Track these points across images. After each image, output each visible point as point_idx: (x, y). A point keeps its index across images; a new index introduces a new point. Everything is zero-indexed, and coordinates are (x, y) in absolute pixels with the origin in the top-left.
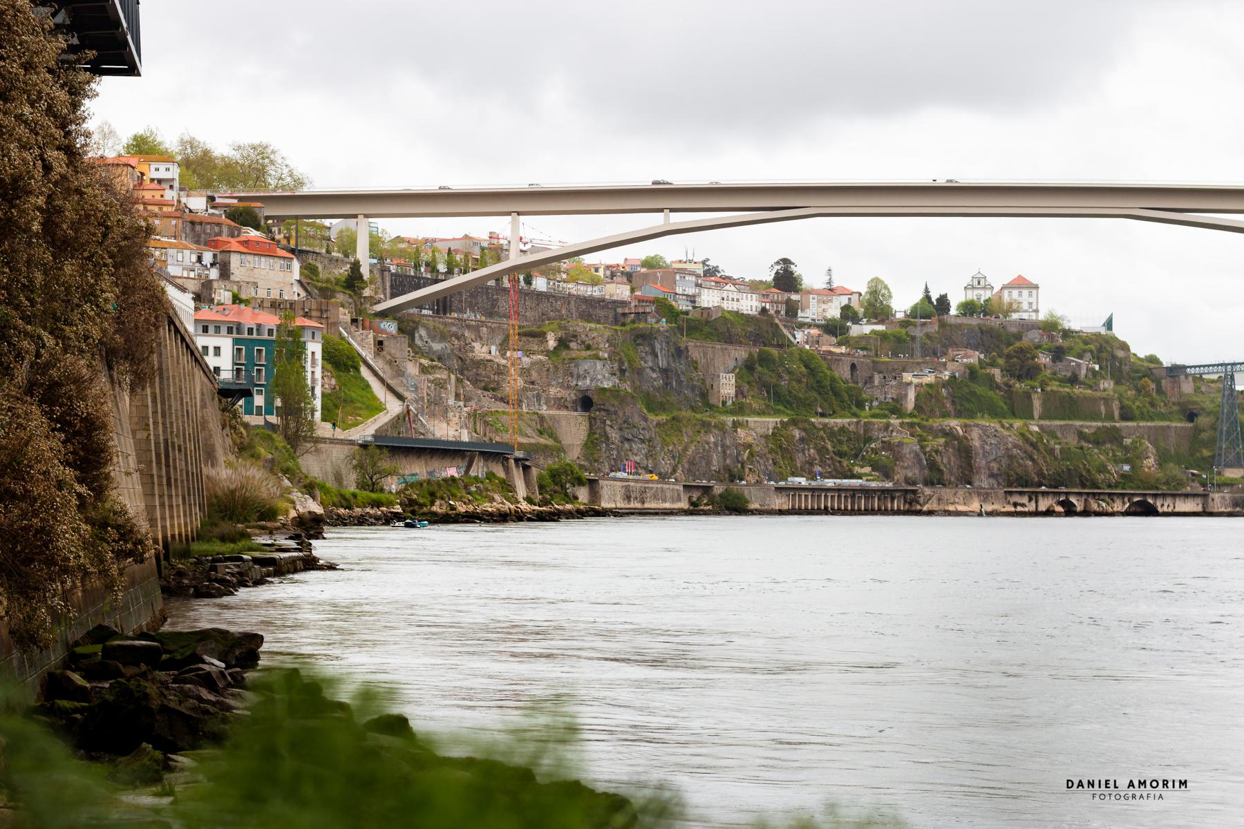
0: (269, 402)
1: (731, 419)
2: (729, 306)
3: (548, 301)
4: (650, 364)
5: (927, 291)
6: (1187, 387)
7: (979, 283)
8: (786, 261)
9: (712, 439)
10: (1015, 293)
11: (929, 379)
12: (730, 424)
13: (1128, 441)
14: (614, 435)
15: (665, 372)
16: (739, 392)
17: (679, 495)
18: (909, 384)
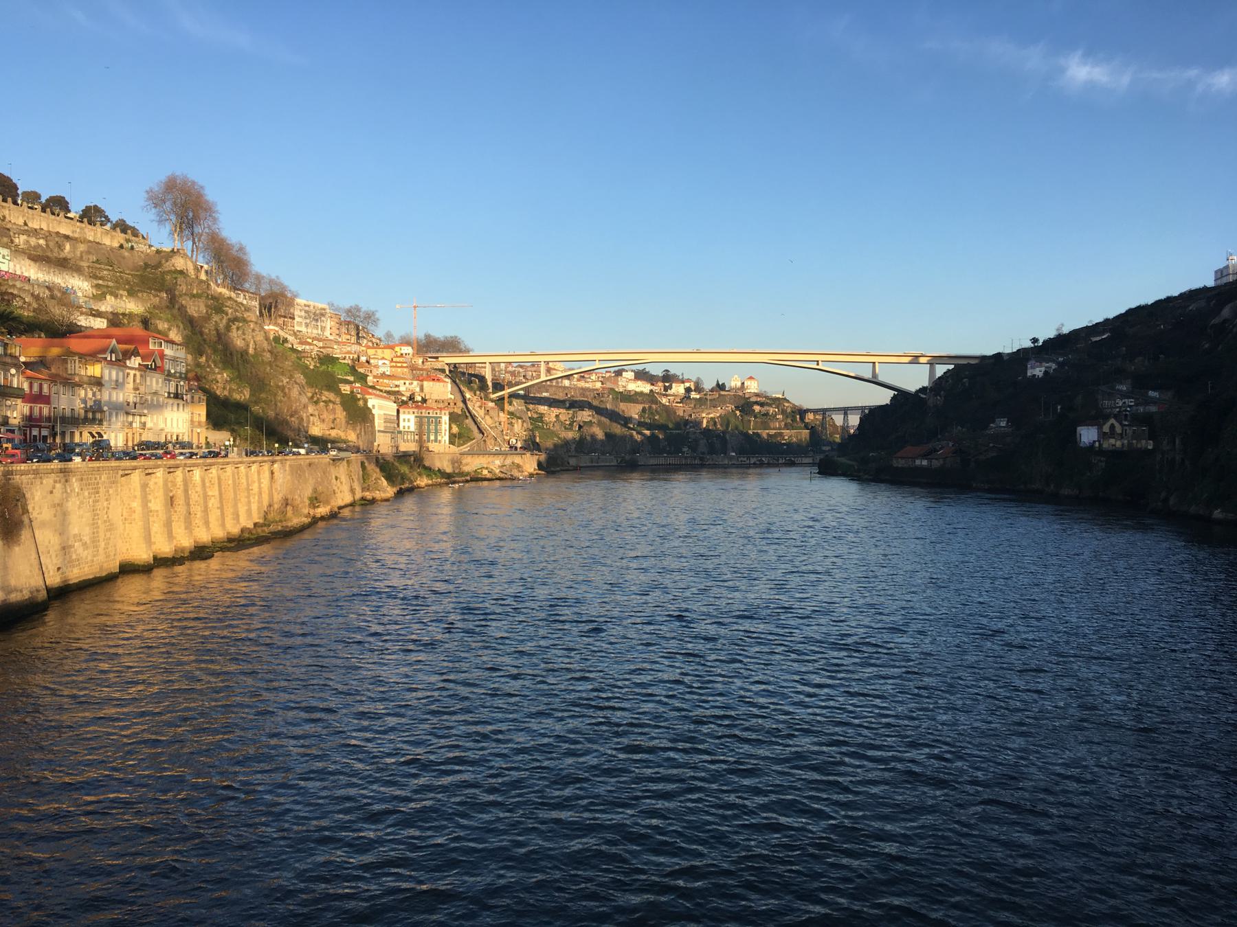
2: (638, 390)
8: (667, 371)
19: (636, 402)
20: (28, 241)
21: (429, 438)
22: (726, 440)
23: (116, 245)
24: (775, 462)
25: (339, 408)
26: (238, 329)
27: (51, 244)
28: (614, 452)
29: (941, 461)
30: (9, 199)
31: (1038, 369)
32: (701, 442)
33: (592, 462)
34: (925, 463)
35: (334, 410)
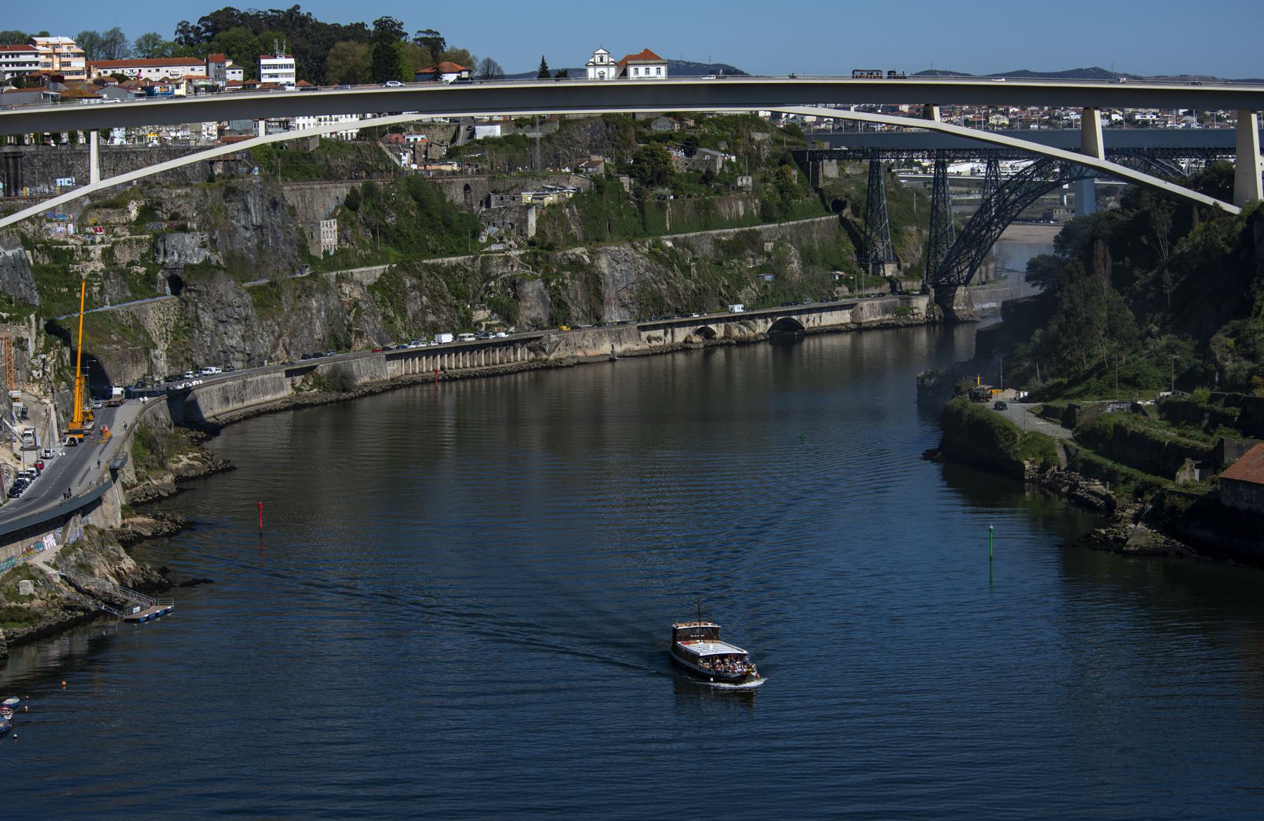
1: (335, 273)
3: (128, 158)
4: (243, 222)
5: (544, 64)
6: (830, 170)
7: (602, 60)
9: (315, 304)
10: (642, 70)
11: (551, 198)
12: (333, 280)
13: (769, 246)
14: (207, 319)
15: (259, 228)
16: (342, 236)
17: (281, 383)
18: (529, 206)
19: (330, 176)
33: (226, 400)
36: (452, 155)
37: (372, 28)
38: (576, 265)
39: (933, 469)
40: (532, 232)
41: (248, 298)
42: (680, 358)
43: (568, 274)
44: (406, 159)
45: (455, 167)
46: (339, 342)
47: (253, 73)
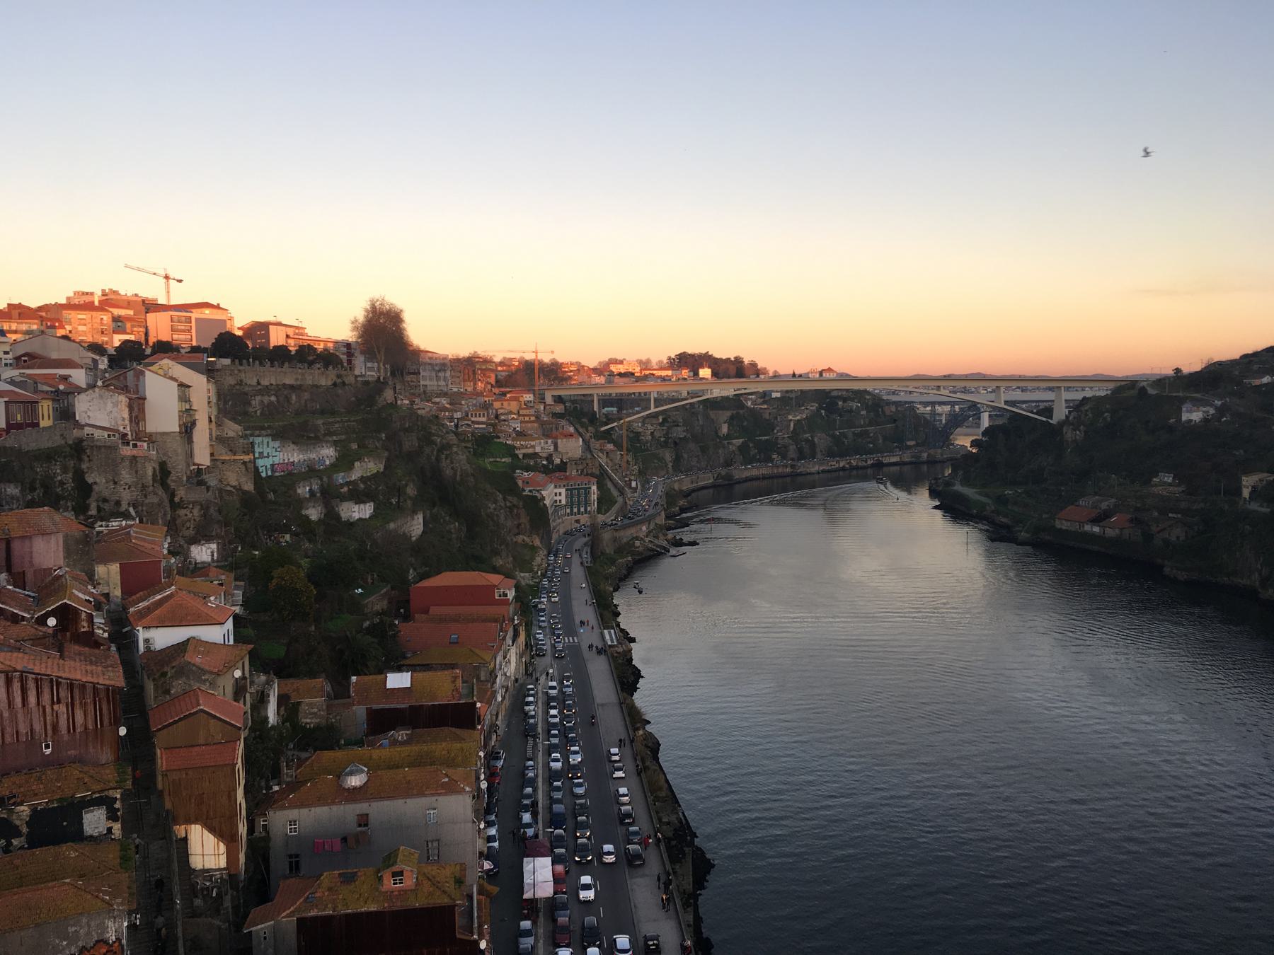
0: (579, 510)
14: (685, 456)
18: (791, 420)
19: (723, 408)
20: (262, 401)
21: (579, 510)
22: (814, 444)
23: (330, 383)
24: (864, 463)
25: (523, 512)
26: (446, 458)
27: (281, 399)
28: (709, 467)
29: (1117, 531)
30: (244, 361)
31: (1195, 414)
32: (791, 447)
33: (692, 483)
34: (1096, 529)
35: (518, 516)
36: (765, 402)
37: (733, 359)
38: (807, 440)
39: (939, 513)
40: (792, 429)
41: (699, 449)
42: (841, 473)
43: (804, 443)
44: (749, 403)
45: (766, 407)
46: (728, 464)
47: (696, 374)
